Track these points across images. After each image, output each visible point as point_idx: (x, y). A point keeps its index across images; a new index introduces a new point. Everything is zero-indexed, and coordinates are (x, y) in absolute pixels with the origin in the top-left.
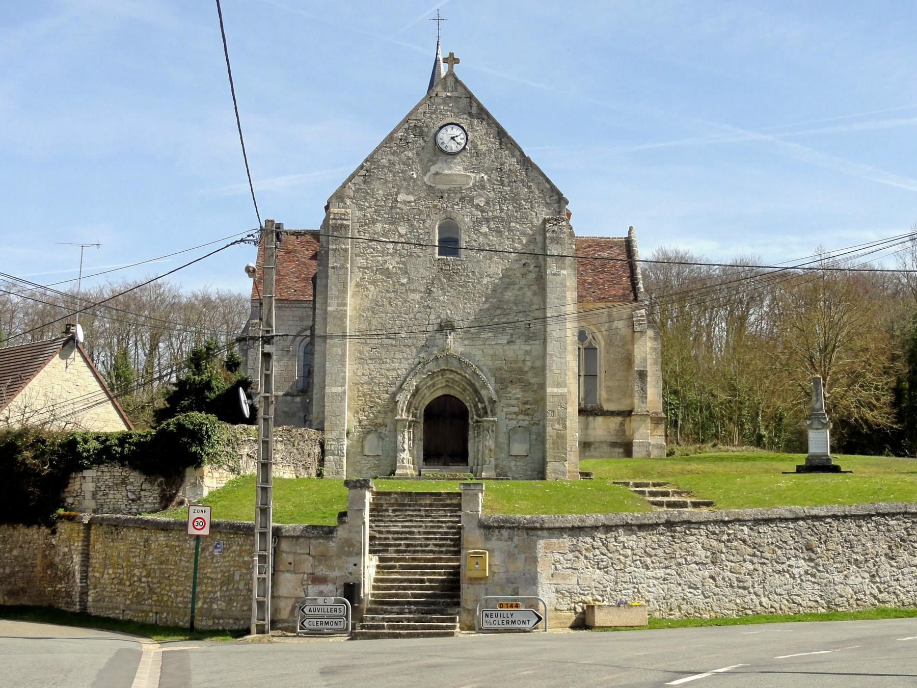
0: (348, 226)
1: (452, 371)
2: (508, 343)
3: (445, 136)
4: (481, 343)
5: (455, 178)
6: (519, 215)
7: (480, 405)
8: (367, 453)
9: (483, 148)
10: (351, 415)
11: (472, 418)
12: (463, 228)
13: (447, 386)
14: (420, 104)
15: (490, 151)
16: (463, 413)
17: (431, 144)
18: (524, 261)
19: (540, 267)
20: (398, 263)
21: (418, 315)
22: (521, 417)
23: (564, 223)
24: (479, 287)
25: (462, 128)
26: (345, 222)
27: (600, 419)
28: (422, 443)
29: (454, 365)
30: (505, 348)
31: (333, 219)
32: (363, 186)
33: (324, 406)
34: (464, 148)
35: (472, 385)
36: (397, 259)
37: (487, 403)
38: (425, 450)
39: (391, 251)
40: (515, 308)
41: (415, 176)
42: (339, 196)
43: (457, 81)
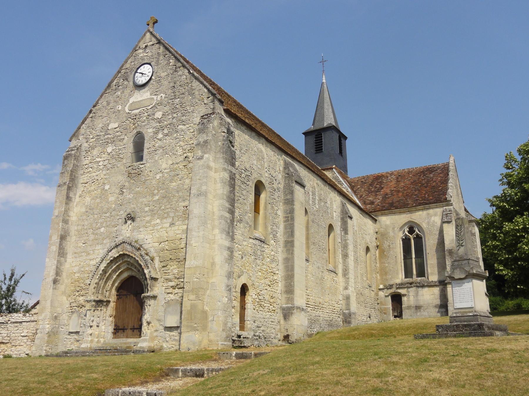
2: (170, 226)
4: (151, 228)
6: (184, 118)
9: (163, 75)
12: (146, 138)
13: (127, 269)
17: (131, 83)
18: (185, 155)
21: (113, 213)
22: (177, 290)
24: (154, 182)
27: (426, 289)
30: (168, 229)
34: (151, 79)
38: (115, 325)
40: (177, 195)
41: (120, 108)
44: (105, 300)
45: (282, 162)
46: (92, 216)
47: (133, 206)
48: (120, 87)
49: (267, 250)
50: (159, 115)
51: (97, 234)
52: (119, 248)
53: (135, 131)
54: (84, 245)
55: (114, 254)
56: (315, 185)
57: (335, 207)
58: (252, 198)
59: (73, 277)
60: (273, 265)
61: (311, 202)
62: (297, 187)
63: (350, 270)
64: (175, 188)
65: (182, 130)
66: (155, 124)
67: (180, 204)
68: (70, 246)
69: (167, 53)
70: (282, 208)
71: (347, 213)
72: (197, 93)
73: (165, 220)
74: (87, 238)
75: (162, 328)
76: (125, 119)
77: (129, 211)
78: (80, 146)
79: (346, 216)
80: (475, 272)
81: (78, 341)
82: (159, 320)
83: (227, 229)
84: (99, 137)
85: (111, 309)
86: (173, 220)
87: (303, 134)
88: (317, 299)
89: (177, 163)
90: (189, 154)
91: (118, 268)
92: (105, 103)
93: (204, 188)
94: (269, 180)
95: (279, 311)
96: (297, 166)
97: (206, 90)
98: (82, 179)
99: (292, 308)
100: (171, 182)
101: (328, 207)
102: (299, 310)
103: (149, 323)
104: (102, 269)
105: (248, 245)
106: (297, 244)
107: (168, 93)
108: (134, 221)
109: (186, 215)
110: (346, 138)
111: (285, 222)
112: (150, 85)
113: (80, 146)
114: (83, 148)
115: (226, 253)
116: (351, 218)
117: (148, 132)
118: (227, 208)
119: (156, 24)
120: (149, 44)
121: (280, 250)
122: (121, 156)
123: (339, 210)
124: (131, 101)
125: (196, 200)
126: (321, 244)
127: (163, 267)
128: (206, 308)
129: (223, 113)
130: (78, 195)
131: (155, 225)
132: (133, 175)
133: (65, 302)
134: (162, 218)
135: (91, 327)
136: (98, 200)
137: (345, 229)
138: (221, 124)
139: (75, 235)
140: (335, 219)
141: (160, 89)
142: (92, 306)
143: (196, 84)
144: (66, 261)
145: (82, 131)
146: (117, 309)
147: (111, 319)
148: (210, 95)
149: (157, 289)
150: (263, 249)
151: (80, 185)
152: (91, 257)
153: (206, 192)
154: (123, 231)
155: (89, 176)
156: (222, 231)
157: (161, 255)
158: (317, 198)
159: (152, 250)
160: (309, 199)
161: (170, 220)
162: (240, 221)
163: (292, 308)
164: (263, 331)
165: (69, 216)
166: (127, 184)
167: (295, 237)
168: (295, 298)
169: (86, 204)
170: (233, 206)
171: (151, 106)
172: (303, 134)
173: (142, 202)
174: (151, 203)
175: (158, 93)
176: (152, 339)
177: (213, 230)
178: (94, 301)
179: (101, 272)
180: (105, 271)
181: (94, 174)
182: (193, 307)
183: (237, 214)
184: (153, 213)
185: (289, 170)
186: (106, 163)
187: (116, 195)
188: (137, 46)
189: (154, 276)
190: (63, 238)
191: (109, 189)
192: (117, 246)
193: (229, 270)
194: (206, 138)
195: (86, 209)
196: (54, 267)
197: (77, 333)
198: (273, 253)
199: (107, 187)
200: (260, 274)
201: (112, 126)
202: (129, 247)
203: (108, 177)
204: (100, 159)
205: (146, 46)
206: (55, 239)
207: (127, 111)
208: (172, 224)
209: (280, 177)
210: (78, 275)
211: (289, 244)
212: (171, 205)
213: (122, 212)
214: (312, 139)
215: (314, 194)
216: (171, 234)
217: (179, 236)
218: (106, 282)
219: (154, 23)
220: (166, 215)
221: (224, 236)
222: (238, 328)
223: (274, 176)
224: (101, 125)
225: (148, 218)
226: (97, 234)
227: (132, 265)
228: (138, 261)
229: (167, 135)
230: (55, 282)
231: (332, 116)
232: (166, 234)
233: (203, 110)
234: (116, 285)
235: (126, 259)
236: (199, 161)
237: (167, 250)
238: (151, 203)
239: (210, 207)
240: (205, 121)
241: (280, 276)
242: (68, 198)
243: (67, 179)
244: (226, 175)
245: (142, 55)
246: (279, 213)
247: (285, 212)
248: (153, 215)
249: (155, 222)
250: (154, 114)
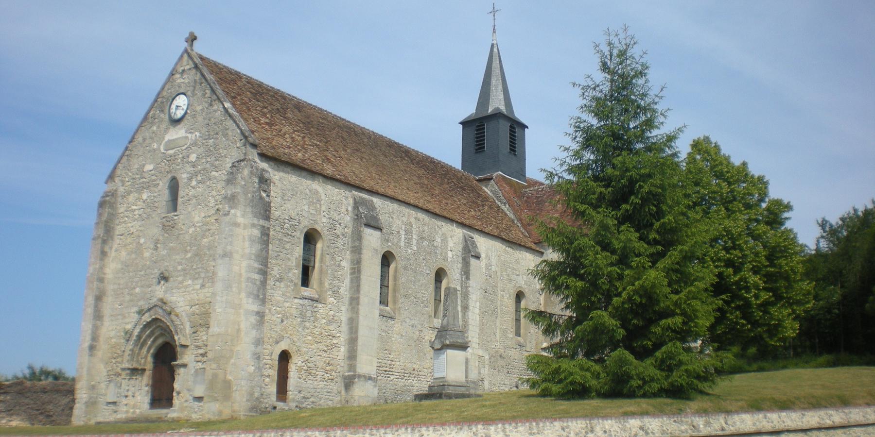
4: (183, 290)
13: (162, 335)
14: (165, 84)
15: (202, 110)
17: (167, 117)
21: (148, 271)
34: (186, 113)
42: (111, 177)
44: (140, 368)
45: (351, 201)
47: (166, 264)
49: (321, 309)
50: (193, 157)
51: (131, 295)
52: (152, 312)
53: (170, 176)
55: (147, 318)
56: (413, 220)
57: (451, 244)
58: (298, 251)
60: (332, 328)
61: (402, 244)
62: (368, 231)
63: (470, 327)
65: (215, 178)
66: (189, 168)
68: (107, 308)
69: (204, 81)
70: (349, 257)
71: (470, 252)
72: (230, 134)
75: (191, 398)
76: (160, 160)
77: (163, 269)
78: (116, 191)
79: (470, 253)
80: (448, 342)
81: (116, 412)
82: (189, 390)
83: (255, 292)
87: (460, 123)
88: (409, 365)
90: (220, 206)
91: (152, 333)
92: (140, 139)
93: (229, 248)
94: (328, 225)
95: (339, 379)
96: (377, 201)
97: (239, 131)
98: (119, 229)
99: (354, 377)
100: (203, 236)
101: (436, 247)
102: (362, 379)
103: (178, 393)
105: (293, 305)
106: (364, 300)
107: (203, 132)
109: (212, 278)
110: (524, 127)
111: (351, 274)
112: (185, 121)
113: (116, 191)
114: (119, 193)
115: (253, 319)
116: (478, 257)
117: (183, 177)
118: (255, 268)
119: (195, 42)
121: (343, 308)
122: (156, 205)
123: (460, 247)
124: (166, 139)
126: (419, 295)
127: (194, 333)
128: (229, 377)
129: (257, 159)
130: (114, 249)
131: (187, 286)
132: (168, 227)
133: (102, 370)
135: (126, 396)
137: (466, 272)
138: (251, 172)
140: (449, 260)
142: (127, 374)
143: (229, 123)
144: (102, 325)
145: (118, 172)
147: (147, 388)
149: (187, 357)
150: (316, 310)
151: (116, 237)
152: (127, 320)
153: (231, 253)
156: (249, 294)
158: (415, 237)
159: (183, 314)
160: (400, 240)
161: (200, 281)
162: (280, 280)
163: (354, 377)
164: (313, 402)
165: (105, 274)
167: (362, 292)
168: (358, 365)
170: (266, 266)
172: (460, 123)
176: (182, 409)
177: (239, 293)
178: (129, 369)
179: (134, 338)
180: (139, 337)
181: (129, 225)
182: (215, 376)
183: (275, 271)
185: (358, 210)
187: (151, 251)
188: (174, 69)
189: (183, 343)
190: (99, 298)
192: (149, 310)
193: (258, 336)
194: (234, 191)
196: (90, 332)
197: (114, 403)
198: (332, 313)
199: (142, 241)
200: (310, 338)
201: (149, 167)
202: (160, 311)
205: (183, 71)
206: (91, 300)
207: (162, 150)
208: (203, 286)
209: (348, 219)
211: (354, 302)
213: (156, 271)
214: (473, 132)
215: (408, 232)
216: (201, 296)
218: (141, 348)
219: (192, 41)
221: (250, 300)
222: (274, 398)
223: (337, 219)
224: (136, 166)
225: (180, 279)
227: (165, 331)
229: (199, 182)
230: (92, 348)
231: (502, 97)
233: (235, 155)
234: (152, 351)
239: (236, 269)
240: (235, 169)
241: (342, 339)
242: (104, 254)
243: (101, 232)
244: (256, 232)
245: (179, 81)
246: (344, 264)
247: (352, 262)
248: (185, 275)
250: (188, 157)
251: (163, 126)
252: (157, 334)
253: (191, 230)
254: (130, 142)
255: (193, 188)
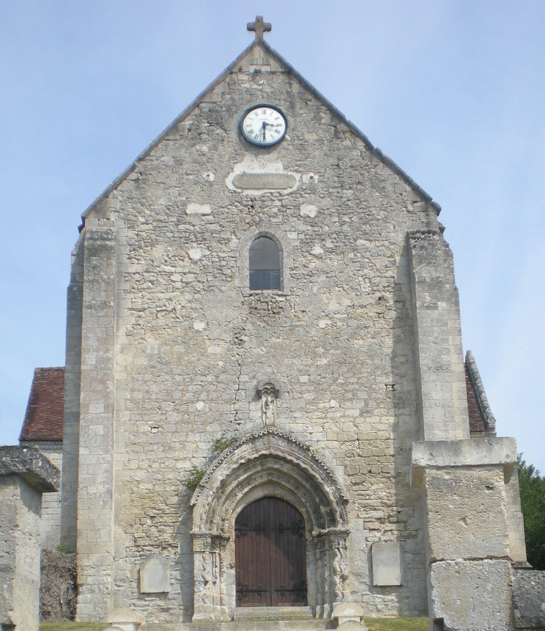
0: (111, 248)
1: (277, 457)
2: (361, 415)
3: (253, 123)
4: (320, 415)
5: (271, 179)
7: (323, 509)
8: (145, 589)
9: (311, 137)
10: (120, 531)
11: (311, 530)
13: (270, 483)
14: (217, 83)
15: (320, 141)
16: (298, 528)
17: (234, 135)
18: (378, 295)
19: (403, 302)
20: (190, 302)
21: (222, 377)
23: (436, 237)
24: (313, 332)
25: (279, 111)
26: (107, 242)
28: (233, 571)
29: (281, 448)
30: (358, 420)
31: (91, 239)
32: (135, 194)
33: (76, 519)
34: (283, 139)
35: (310, 478)
36: (188, 296)
37: (335, 505)
38: (238, 584)
39: (178, 285)
41: (212, 178)
42: (98, 208)
43: (268, 50)
46: (168, 377)
47: (269, 370)
48: (204, 136)
52: (259, 444)
54: (154, 430)
55: (246, 452)
59: (135, 489)
64: (365, 349)
67: (379, 379)
69: (310, 97)
73: (348, 404)
74: (163, 417)
76: (227, 202)
84: (163, 224)
85: (228, 554)
86: (367, 404)
89: (362, 307)
91: (248, 481)
92: (167, 159)
97: (408, 189)
100: (354, 335)
104: (221, 478)
108: (277, 398)
117: (290, 237)
120: (264, 69)
125: (433, 377)
127: (356, 484)
131: (326, 411)
134: (342, 399)
136: (180, 348)
139: (127, 409)
141: (306, 162)
142: (205, 546)
145: (114, 203)
146: (238, 554)
148: (419, 199)
154: (252, 414)
155: (149, 296)
157: (347, 463)
159: (327, 452)
166: (249, 326)
169: (149, 351)
171: (289, 191)
173: (290, 366)
174: (312, 370)
175: (301, 169)
179: (218, 484)
180: (224, 484)
181: (162, 296)
184: (321, 387)
186: (190, 278)
188: (235, 64)
191: (204, 329)
194: (434, 274)
195: (150, 361)
202: (282, 444)
203: (198, 306)
204: (173, 269)
205: (257, 72)
208: (365, 412)
210: (150, 486)
212: (359, 378)
217: (385, 434)
220: (349, 395)
224: (163, 201)
226: (187, 412)
228: (306, 469)
232: (355, 429)
234: (239, 510)
235: (270, 465)
236: (429, 311)
237: (359, 455)
238: (312, 370)
245: (247, 85)
249: (327, 405)
250: (298, 207)
251: (227, 150)
252: (259, 481)
253: (322, 324)
254: (141, 159)
255: (318, 257)
